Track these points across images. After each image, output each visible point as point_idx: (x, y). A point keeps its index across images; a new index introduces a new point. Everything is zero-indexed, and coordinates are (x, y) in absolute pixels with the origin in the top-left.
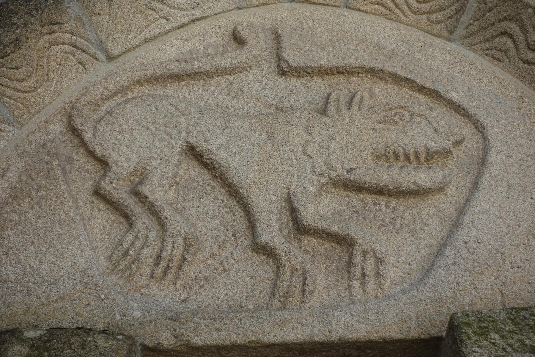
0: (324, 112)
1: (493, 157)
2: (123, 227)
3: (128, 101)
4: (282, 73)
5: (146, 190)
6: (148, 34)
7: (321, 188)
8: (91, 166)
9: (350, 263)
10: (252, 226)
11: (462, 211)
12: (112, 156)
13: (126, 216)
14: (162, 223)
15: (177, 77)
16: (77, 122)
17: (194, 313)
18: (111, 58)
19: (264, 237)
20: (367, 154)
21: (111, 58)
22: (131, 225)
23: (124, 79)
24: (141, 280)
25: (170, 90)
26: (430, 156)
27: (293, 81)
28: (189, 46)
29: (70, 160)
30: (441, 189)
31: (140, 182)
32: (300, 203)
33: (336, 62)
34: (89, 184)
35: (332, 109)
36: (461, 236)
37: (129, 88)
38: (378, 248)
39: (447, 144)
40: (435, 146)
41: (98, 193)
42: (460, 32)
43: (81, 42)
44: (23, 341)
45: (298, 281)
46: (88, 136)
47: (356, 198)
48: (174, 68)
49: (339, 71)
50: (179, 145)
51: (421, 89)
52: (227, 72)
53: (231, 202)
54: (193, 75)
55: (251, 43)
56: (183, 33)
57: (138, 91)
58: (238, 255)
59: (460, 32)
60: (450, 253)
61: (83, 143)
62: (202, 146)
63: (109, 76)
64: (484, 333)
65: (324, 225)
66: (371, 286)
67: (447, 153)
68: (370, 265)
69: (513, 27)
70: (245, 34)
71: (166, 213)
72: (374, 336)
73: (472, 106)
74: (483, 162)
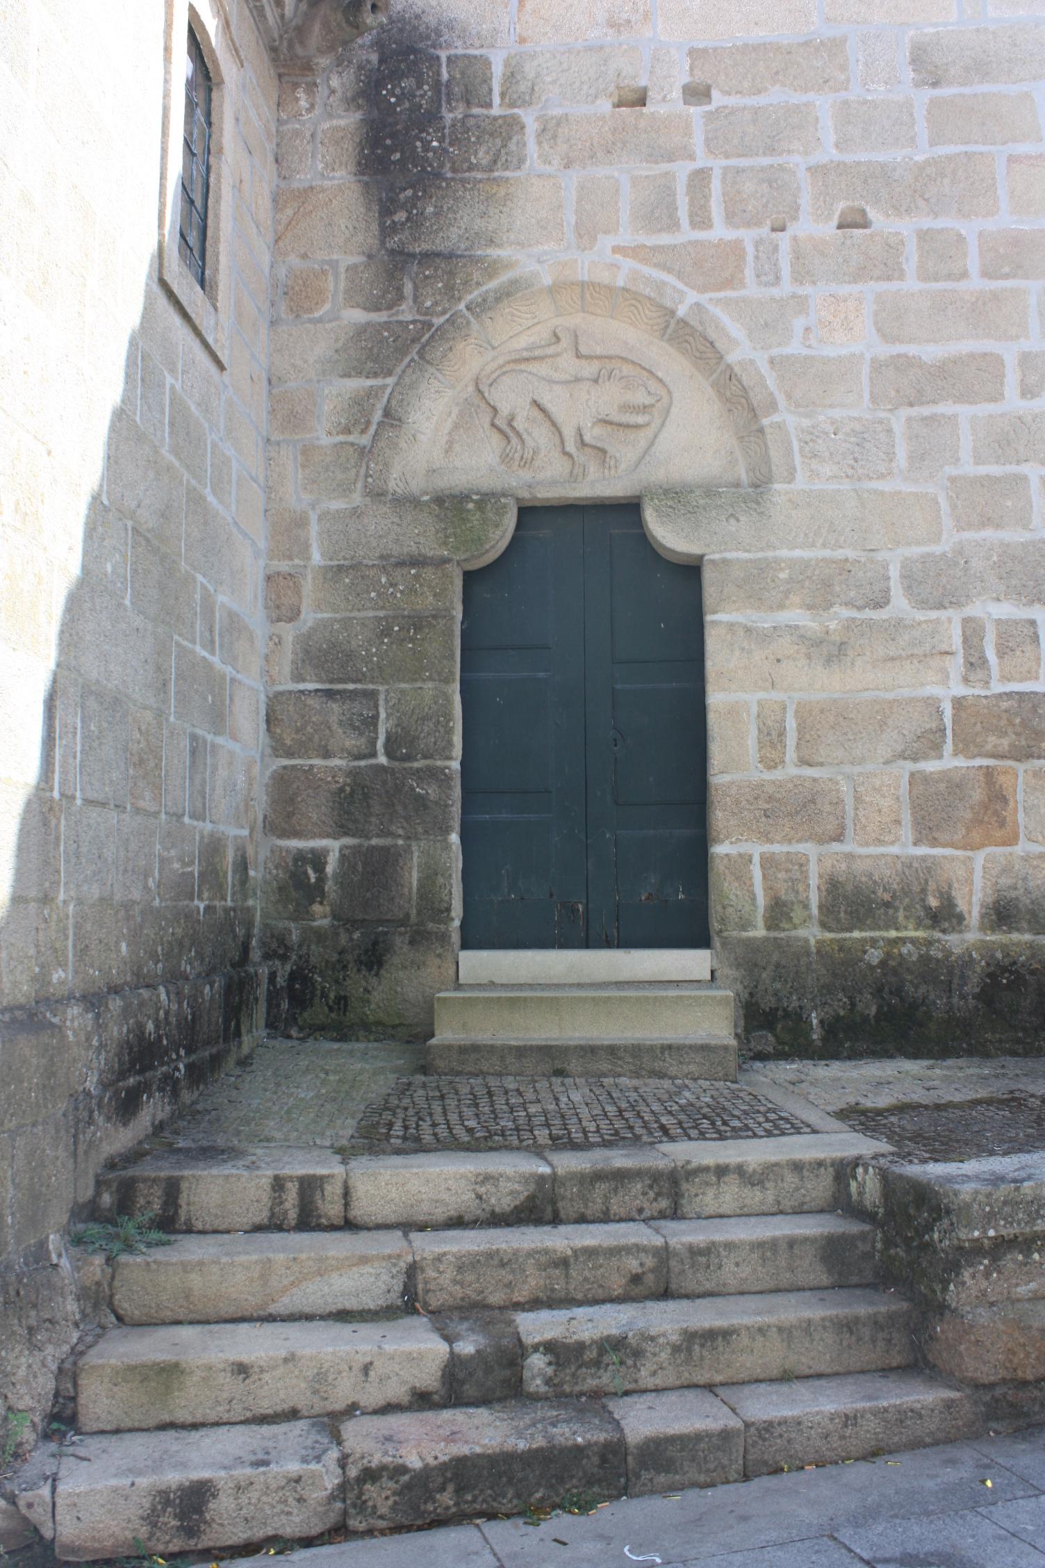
0: (596, 381)
1: (674, 410)
2: (505, 442)
3: (504, 373)
4: (578, 357)
5: (515, 424)
6: (511, 334)
7: (594, 424)
8: (489, 410)
9: (604, 461)
10: (562, 442)
11: (655, 437)
12: (498, 405)
13: (507, 438)
14: (523, 441)
15: (527, 360)
16: (481, 387)
17: (538, 483)
18: (494, 348)
19: (568, 449)
20: (615, 407)
21: (494, 348)
22: (509, 442)
23: (501, 361)
24: (515, 467)
25: (523, 366)
26: (645, 407)
27: (584, 362)
28: (532, 339)
29: (479, 406)
30: (648, 425)
31: (512, 419)
32: (584, 432)
33: (605, 353)
34: (488, 420)
35: (601, 380)
36: (653, 450)
37: (504, 366)
38: (618, 455)
39: (653, 401)
40: (647, 403)
41: (493, 425)
42: (667, 337)
43: (480, 342)
44: (472, 501)
45: (581, 470)
46: (486, 395)
47: (609, 428)
48: (525, 354)
49: (606, 357)
50: (529, 400)
51: (644, 369)
52: (551, 356)
53: (553, 429)
54: (535, 358)
55: (563, 340)
56: (529, 332)
57: (508, 368)
58: (557, 455)
59: (667, 337)
60: (647, 458)
61: (484, 397)
62: (540, 401)
63: (494, 359)
64: (652, 499)
65: (594, 443)
66: (613, 472)
67: (653, 406)
68: (612, 463)
69: (691, 339)
70: (560, 335)
71: (525, 436)
72: (612, 495)
73: (667, 380)
74: (668, 411)
